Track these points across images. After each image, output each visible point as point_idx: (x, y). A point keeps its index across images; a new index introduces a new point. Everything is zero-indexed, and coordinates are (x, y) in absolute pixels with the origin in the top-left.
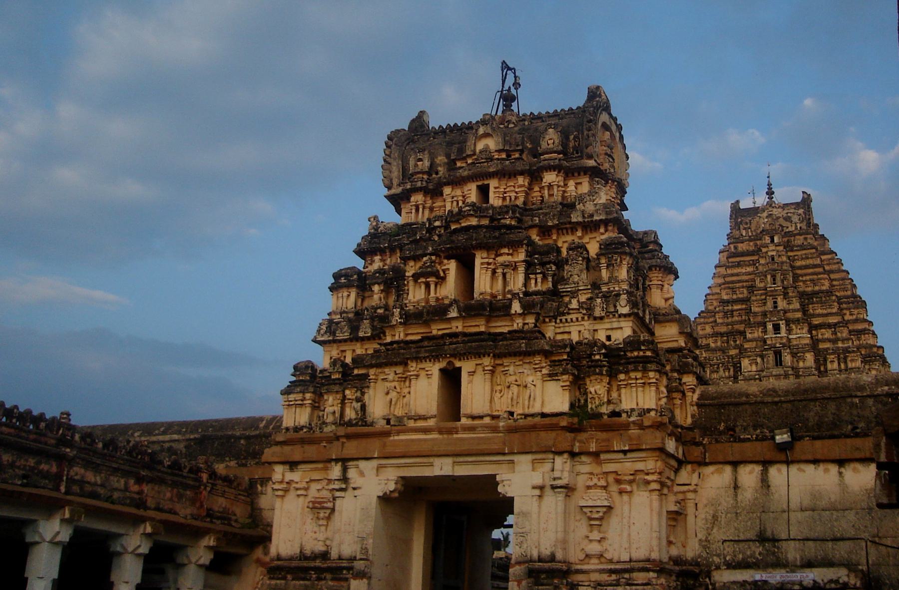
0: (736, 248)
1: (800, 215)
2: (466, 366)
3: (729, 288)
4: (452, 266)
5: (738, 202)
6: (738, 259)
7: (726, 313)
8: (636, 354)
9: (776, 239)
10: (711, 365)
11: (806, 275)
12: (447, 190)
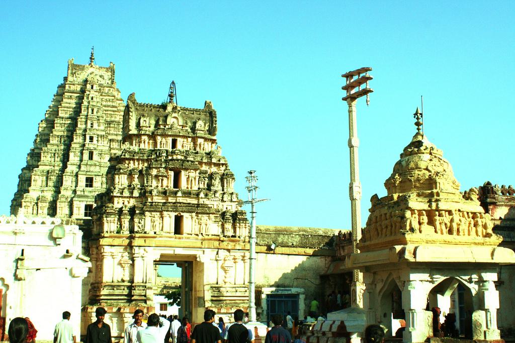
2: (186, 215)
3: (64, 110)
4: (172, 173)
6: (70, 94)
8: (241, 217)
11: (108, 111)
12: (159, 139)
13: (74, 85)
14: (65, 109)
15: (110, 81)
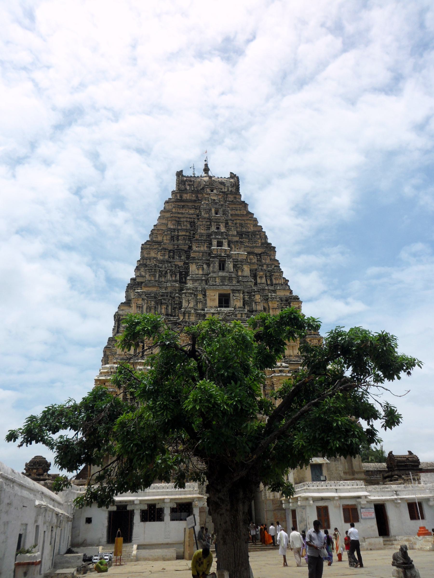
0: (181, 197)
1: (231, 182)
3: (176, 220)
5: (182, 171)
6: (183, 204)
9: (215, 191)
10: (160, 271)
15: (235, 188)
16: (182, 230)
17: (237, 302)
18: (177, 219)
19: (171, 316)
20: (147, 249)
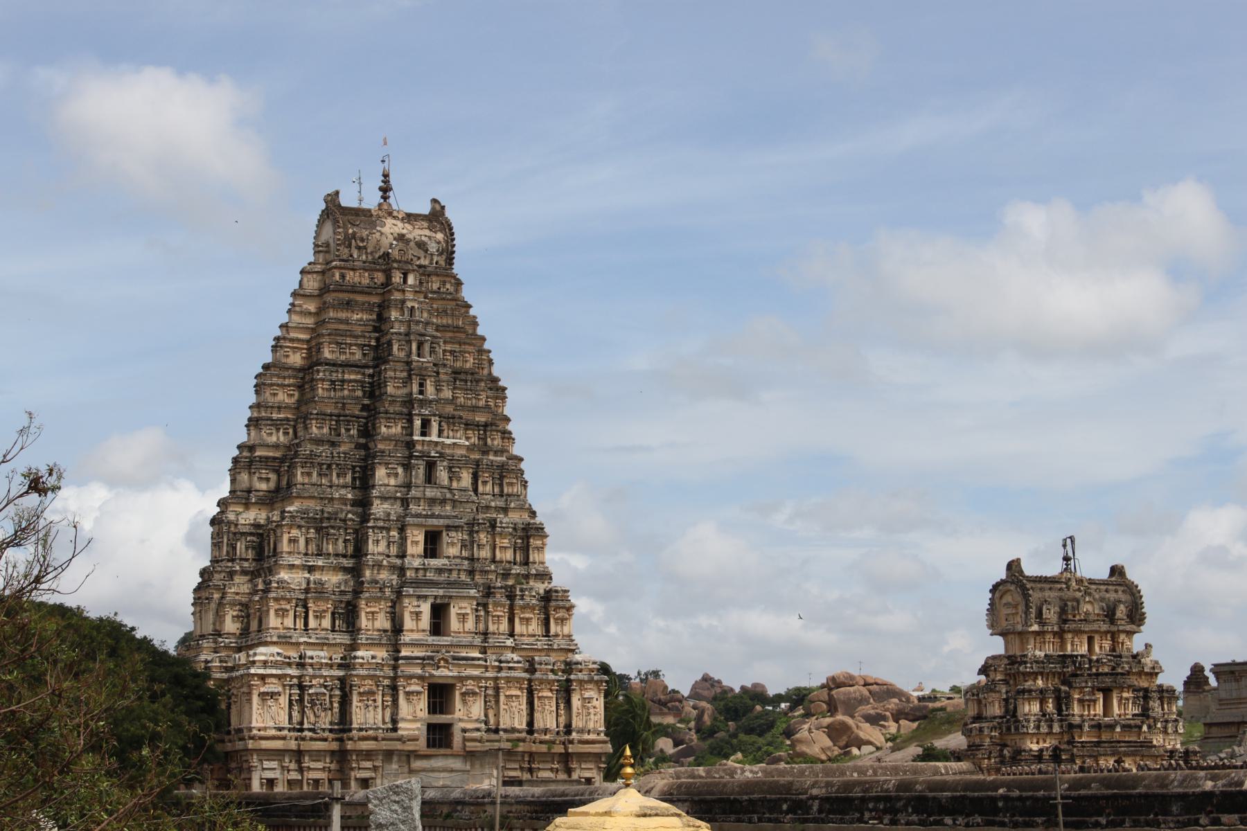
0: (343, 276)
1: (439, 243)
4: (1100, 696)
6: (346, 296)
7: (333, 382)
10: (321, 465)
13: (353, 270)
14: (340, 339)
16: (347, 365)
17: (452, 548)
18: (340, 339)
19: (344, 556)
20: (272, 385)
